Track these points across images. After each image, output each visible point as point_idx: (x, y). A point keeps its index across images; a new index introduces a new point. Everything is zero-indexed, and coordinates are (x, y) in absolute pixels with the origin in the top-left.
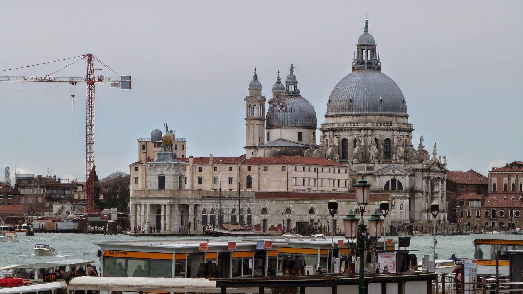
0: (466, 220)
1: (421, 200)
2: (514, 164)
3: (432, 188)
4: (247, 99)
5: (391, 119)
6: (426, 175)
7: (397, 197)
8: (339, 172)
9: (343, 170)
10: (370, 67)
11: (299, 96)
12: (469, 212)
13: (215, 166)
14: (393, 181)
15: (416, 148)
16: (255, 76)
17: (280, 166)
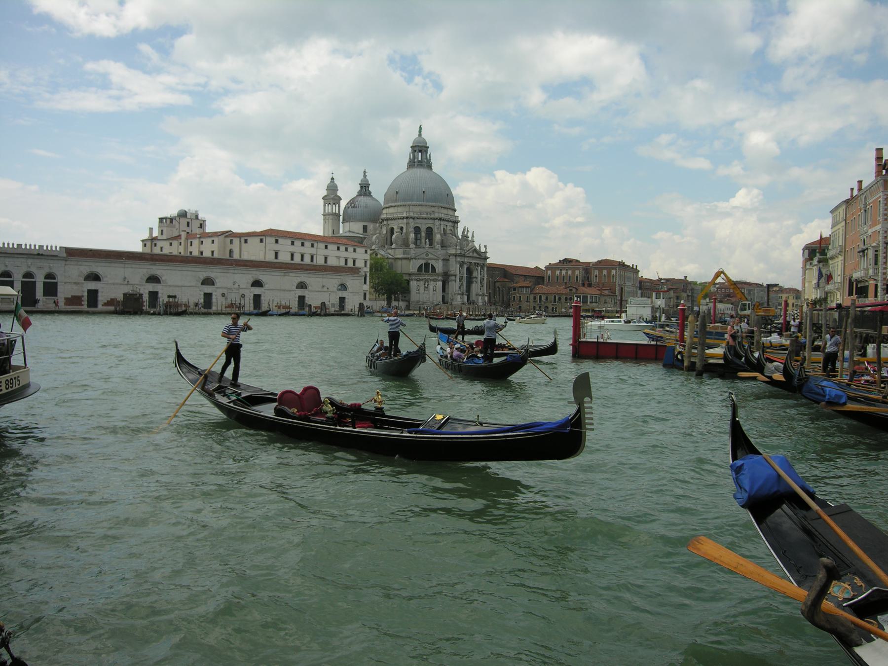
0: (518, 304)
1: (454, 282)
2: (566, 259)
3: (470, 272)
4: (323, 198)
5: (433, 209)
6: (459, 259)
7: (431, 280)
8: (355, 250)
9: (360, 250)
10: (422, 165)
11: (372, 196)
12: (520, 297)
13: (202, 240)
14: (427, 265)
15: (460, 237)
16: (332, 179)
17: (258, 239)
